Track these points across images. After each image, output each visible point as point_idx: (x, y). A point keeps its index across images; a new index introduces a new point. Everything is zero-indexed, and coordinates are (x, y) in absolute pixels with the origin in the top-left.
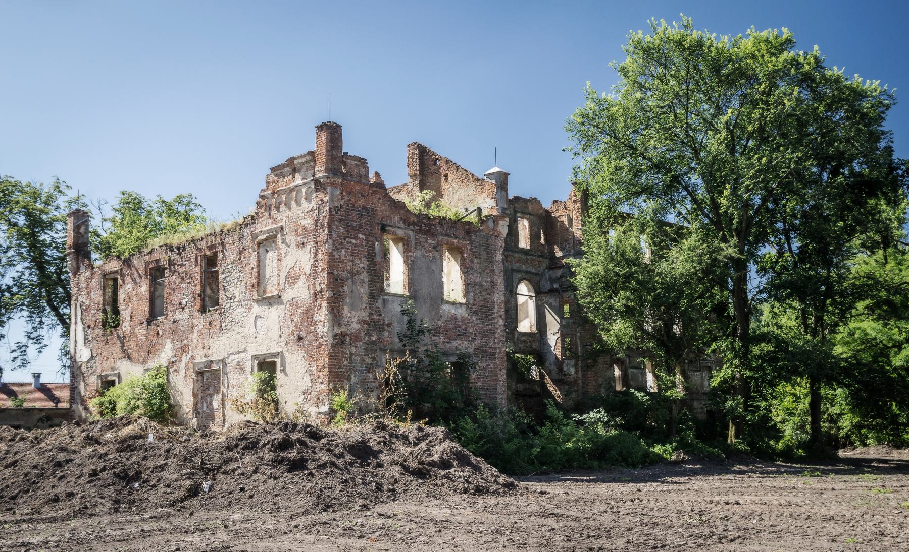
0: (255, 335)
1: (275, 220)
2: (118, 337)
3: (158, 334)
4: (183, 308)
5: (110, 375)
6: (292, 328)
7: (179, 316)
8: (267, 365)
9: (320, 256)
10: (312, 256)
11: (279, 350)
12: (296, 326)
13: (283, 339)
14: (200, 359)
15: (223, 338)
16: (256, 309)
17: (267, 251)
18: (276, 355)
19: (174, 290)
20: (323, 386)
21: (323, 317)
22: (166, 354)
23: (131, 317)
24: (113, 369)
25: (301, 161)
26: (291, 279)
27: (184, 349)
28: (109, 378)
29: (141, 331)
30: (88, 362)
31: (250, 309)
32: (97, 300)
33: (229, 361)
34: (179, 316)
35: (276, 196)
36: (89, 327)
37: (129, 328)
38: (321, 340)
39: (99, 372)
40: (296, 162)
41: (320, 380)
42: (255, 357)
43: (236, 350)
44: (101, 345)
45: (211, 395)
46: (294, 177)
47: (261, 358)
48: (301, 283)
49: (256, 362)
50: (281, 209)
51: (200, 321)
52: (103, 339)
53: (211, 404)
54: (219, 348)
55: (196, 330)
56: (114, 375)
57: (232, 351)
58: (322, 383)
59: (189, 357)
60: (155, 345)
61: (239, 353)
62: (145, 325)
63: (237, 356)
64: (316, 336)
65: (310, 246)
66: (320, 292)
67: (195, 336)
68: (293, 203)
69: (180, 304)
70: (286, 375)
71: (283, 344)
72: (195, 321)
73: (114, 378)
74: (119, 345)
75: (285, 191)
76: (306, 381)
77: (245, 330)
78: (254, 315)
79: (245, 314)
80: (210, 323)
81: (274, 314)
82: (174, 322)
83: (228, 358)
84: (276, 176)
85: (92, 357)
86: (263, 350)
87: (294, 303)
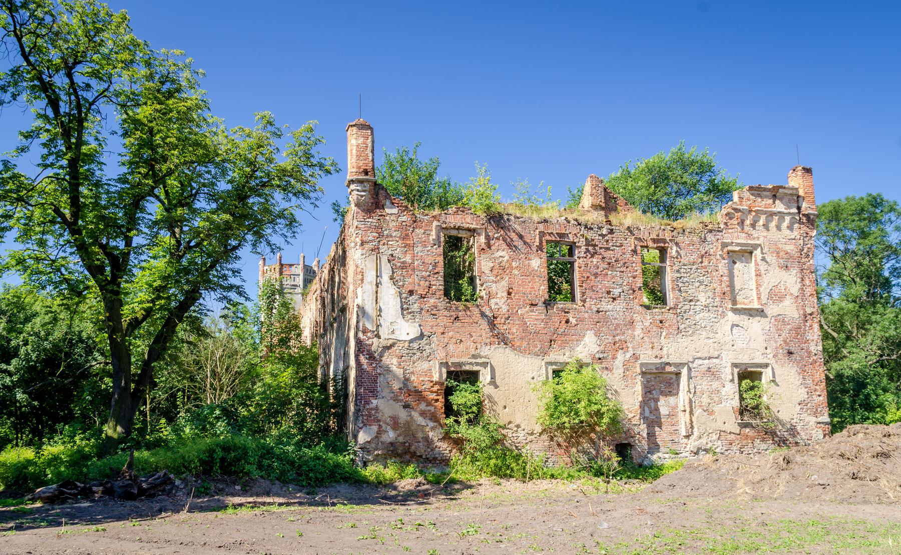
0: (732, 343)
1: (749, 236)
2: (483, 314)
3: (567, 322)
4: (614, 299)
5: (471, 364)
6: (780, 341)
7: (606, 305)
8: (748, 375)
9: (807, 282)
10: (799, 280)
11: (765, 361)
12: (785, 341)
13: (768, 351)
14: (648, 357)
15: (684, 342)
16: (731, 317)
17: (735, 263)
18: (766, 366)
19: (596, 275)
20: (821, 398)
21: (816, 337)
22: (588, 345)
23: (509, 294)
24: (474, 357)
25: (786, 191)
26: (776, 296)
27: (620, 346)
28: (467, 368)
29: (535, 318)
30: (411, 341)
31: (723, 315)
32: (430, 260)
33: (695, 365)
34: (606, 305)
35: (754, 214)
36: (411, 293)
37: (504, 309)
38: (815, 358)
39: (441, 355)
40: (781, 190)
41: (818, 393)
42: (735, 365)
43: (707, 355)
44: (443, 321)
45: (657, 400)
46: (774, 203)
47: (743, 367)
48: (788, 302)
49: (736, 370)
50: (757, 228)
51: (644, 320)
52: (446, 313)
53: (657, 409)
54: (674, 350)
55: (639, 326)
57: (699, 355)
58: (819, 396)
59: (628, 355)
60: (564, 334)
61: (710, 358)
62: (541, 307)
63: (706, 361)
64: (809, 353)
65: (794, 272)
66: (811, 314)
67: (638, 332)
68: (773, 224)
69: (609, 293)
71: (770, 356)
72: (637, 317)
73: (475, 368)
74: (484, 324)
75: (765, 213)
76: (802, 394)
77: (717, 336)
78: (730, 323)
79: (716, 320)
80: (661, 322)
81: (756, 325)
82: (598, 312)
83: (693, 362)
84: (752, 194)
85: (422, 336)
86: (745, 359)
87: (780, 320)
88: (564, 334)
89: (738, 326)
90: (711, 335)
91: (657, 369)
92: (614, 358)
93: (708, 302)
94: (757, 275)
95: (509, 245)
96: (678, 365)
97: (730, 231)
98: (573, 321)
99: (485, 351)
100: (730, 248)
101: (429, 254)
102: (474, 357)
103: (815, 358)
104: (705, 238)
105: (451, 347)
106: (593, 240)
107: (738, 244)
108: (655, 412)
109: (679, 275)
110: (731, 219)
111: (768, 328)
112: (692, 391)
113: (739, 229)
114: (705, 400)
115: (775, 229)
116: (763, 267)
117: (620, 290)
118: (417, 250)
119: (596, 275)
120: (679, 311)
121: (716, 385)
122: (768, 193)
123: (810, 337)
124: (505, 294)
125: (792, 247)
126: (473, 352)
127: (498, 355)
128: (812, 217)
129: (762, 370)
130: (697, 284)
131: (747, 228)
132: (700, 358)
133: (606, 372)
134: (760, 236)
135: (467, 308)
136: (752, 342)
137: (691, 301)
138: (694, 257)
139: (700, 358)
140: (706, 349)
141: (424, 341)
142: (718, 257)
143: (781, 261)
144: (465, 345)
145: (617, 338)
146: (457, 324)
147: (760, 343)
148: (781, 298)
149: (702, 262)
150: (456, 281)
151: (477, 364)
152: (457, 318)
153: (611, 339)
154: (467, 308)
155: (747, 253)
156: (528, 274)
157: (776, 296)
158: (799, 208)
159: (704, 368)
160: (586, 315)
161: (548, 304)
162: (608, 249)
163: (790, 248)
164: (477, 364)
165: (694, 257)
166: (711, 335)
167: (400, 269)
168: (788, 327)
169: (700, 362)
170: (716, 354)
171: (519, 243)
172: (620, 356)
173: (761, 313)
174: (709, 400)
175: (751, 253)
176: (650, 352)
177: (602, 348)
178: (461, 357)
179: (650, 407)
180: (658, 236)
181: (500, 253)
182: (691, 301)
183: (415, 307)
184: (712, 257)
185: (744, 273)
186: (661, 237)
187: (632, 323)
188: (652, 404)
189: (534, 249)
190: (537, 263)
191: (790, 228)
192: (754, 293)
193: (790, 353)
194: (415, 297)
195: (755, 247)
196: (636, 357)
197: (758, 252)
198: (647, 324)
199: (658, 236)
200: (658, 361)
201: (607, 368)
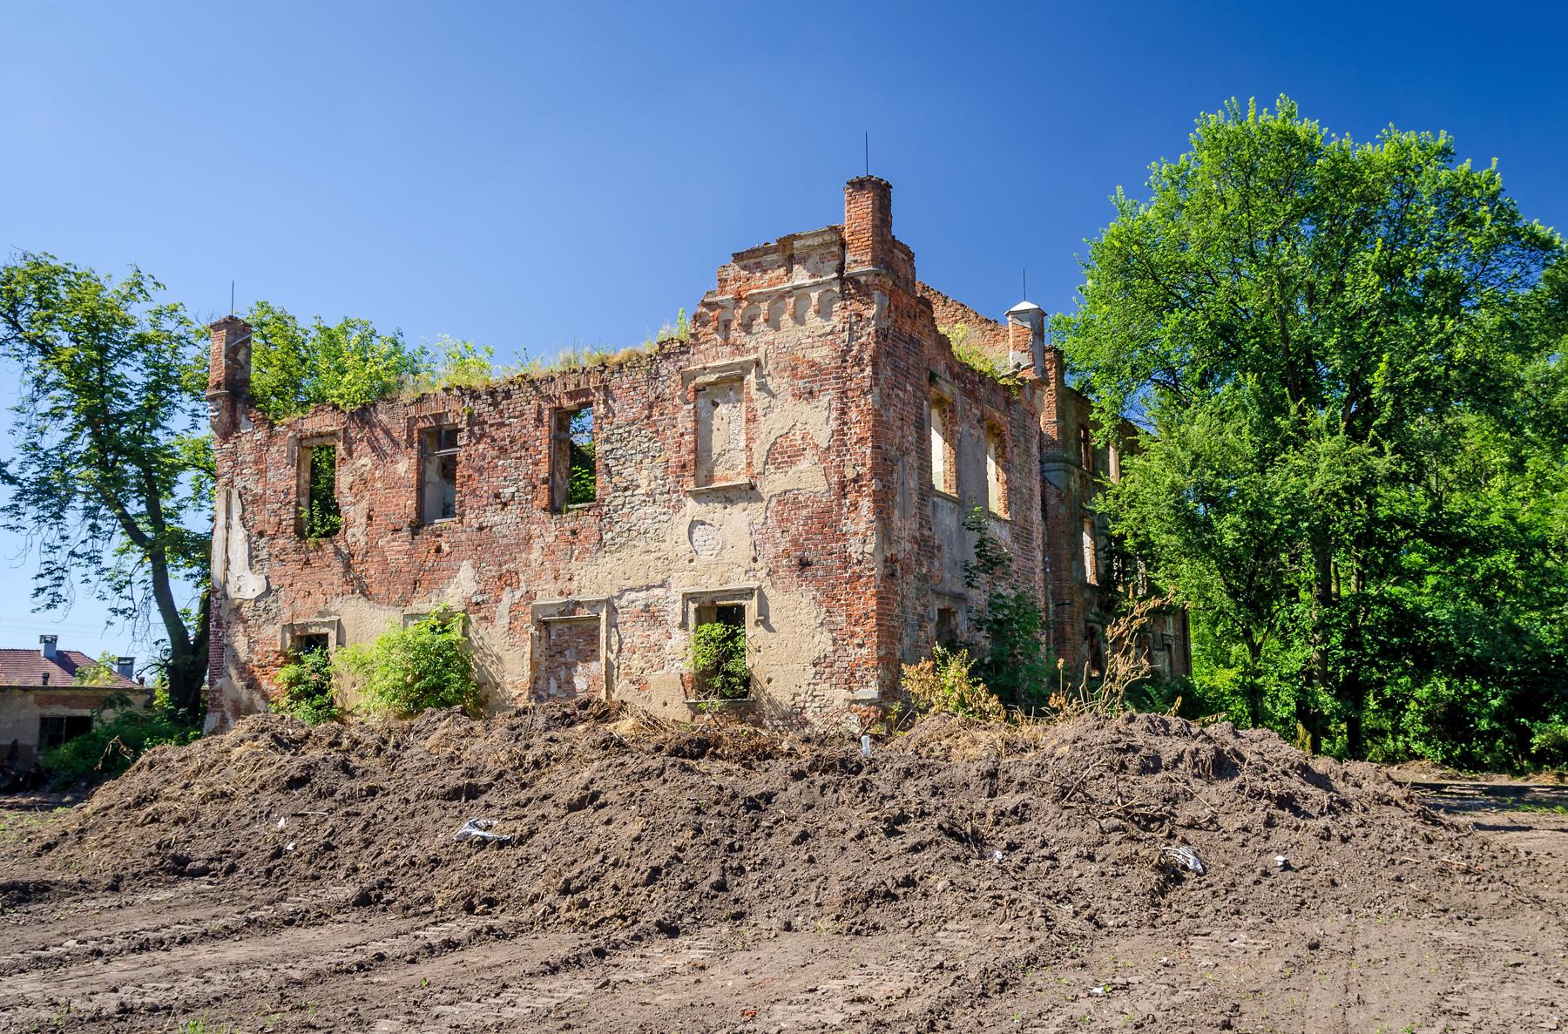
0: (689, 556)
1: (738, 349)
2: (338, 552)
3: (438, 550)
4: (505, 504)
5: (316, 624)
6: (784, 543)
7: (491, 518)
8: (723, 613)
9: (853, 415)
10: (835, 414)
11: (753, 584)
12: (794, 542)
13: (760, 564)
14: (548, 596)
15: (608, 562)
16: (692, 508)
17: (716, 405)
18: (749, 593)
19: (480, 470)
20: (864, 651)
21: (862, 526)
22: (461, 585)
23: (370, 518)
24: (321, 614)
25: (809, 242)
26: (782, 455)
27: (506, 580)
28: (313, 630)
29: (396, 548)
30: (257, 599)
31: (678, 506)
32: (282, 486)
33: (623, 602)
34: (491, 518)
35: (745, 304)
36: (261, 534)
37: (363, 539)
38: (857, 569)
39: (286, 616)
40: (797, 244)
41: (857, 641)
42: (688, 597)
43: (642, 582)
44: (292, 568)
45: (570, 667)
46: (789, 271)
47: (707, 599)
48: (804, 464)
49: (692, 606)
50: (755, 329)
51: (547, 531)
52: (296, 557)
53: (570, 682)
54: (593, 579)
55: (537, 544)
56: (329, 624)
57: (629, 584)
58: (860, 646)
59: (518, 594)
60: (432, 570)
61: (648, 588)
62: (406, 533)
63: (643, 594)
64: (846, 562)
65: (827, 398)
66: (855, 481)
67: (536, 554)
68: (786, 318)
69: (497, 496)
70: (770, 629)
71: (762, 574)
72: (535, 529)
73: (324, 630)
74: (338, 567)
75: (768, 296)
76: (823, 642)
77: (663, 546)
78: (688, 520)
79: (666, 518)
80: (574, 532)
81: (738, 518)
82: (481, 529)
83: (620, 597)
84: (744, 268)
85: (269, 590)
86: (711, 584)
87: (789, 500)
88: (432, 570)
89: (703, 523)
90: (653, 546)
91: (561, 613)
92: (498, 600)
93: (653, 485)
94: (748, 420)
95: (374, 449)
96: (594, 605)
97: (702, 347)
98: (446, 548)
99: (336, 604)
100: (699, 380)
101: (284, 478)
102: (321, 614)
103: (857, 569)
104: (657, 372)
105: (299, 602)
106: (480, 415)
107: (714, 370)
108: (565, 687)
109: (608, 447)
110: (704, 325)
111: (761, 519)
112: (615, 648)
113: (719, 339)
114: (637, 662)
115: (791, 323)
116: (760, 401)
117: (513, 489)
118: (270, 474)
119: (480, 470)
120: (605, 509)
121: (656, 635)
122: (775, 257)
123: (848, 526)
124: (364, 520)
125: (825, 351)
126: (321, 607)
127: (351, 610)
128: (863, 279)
129: (744, 602)
130: (640, 456)
131: (734, 335)
132: (631, 589)
133: (484, 624)
134: (761, 342)
135: (319, 547)
136: (724, 548)
137: (626, 489)
138: (636, 410)
139: (631, 589)
140: (642, 571)
141: (271, 598)
142: (677, 401)
143: (801, 383)
144: (315, 596)
145: (505, 568)
146: (307, 570)
147: (744, 551)
148: (794, 456)
149: (648, 417)
150: (319, 508)
151: (324, 624)
152: (307, 563)
153: (494, 571)
154: (319, 547)
155: (730, 384)
156: (394, 484)
157: (782, 455)
158: (841, 269)
159: (640, 605)
160: (464, 537)
161: (416, 529)
162: (502, 425)
163: (823, 354)
164: (324, 624)
165: (636, 410)
166: (653, 546)
167: (252, 502)
168: (804, 512)
169: (633, 595)
170: (658, 579)
171: (384, 441)
172: (507, 598)
173: (749, 492)
174: (642, 664)
175: (742, 379)
176: (551, 586)
177: (481, 587)
178: (307, 616)
179: (558, 679)
180: (578, 385)
181: (364, 461)
182: (626, 489)
183: (263, 554)
184: (667, 404)
185: (727, 420)
186: (582, 386)
187: (528, 539)
188: (563, 674)
189: (403, 445)
190: (404, 466)
191: (824, 312)
192: (743, 456)
193: (804, 564)
194: (264, 540)
195: (745, 368)
196: (529, 596)
197: (751, 378)
198: (550, 539)
199: (578, 385)
200: (559, 600)
201: (486, 618)
